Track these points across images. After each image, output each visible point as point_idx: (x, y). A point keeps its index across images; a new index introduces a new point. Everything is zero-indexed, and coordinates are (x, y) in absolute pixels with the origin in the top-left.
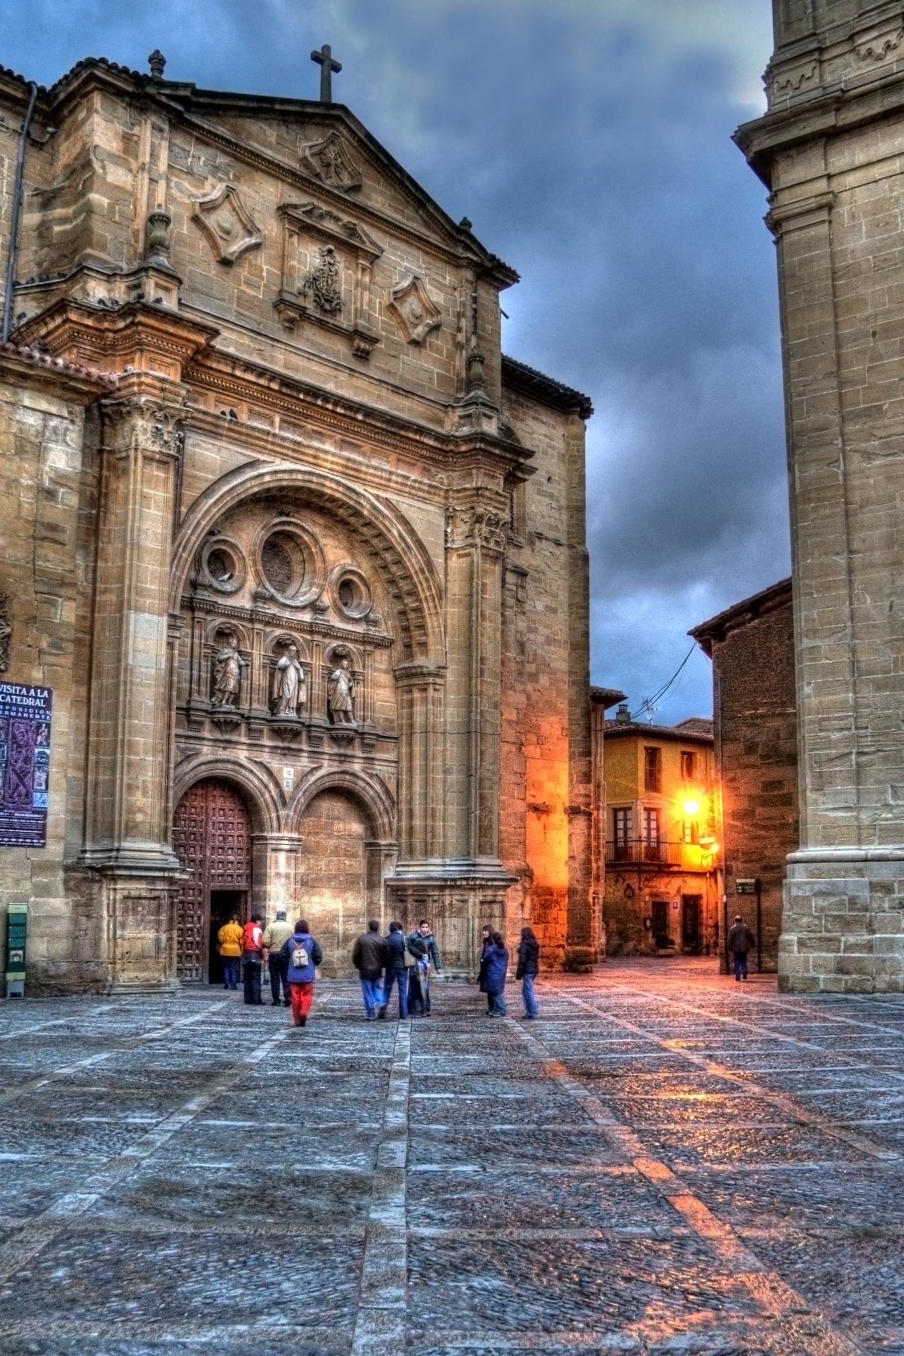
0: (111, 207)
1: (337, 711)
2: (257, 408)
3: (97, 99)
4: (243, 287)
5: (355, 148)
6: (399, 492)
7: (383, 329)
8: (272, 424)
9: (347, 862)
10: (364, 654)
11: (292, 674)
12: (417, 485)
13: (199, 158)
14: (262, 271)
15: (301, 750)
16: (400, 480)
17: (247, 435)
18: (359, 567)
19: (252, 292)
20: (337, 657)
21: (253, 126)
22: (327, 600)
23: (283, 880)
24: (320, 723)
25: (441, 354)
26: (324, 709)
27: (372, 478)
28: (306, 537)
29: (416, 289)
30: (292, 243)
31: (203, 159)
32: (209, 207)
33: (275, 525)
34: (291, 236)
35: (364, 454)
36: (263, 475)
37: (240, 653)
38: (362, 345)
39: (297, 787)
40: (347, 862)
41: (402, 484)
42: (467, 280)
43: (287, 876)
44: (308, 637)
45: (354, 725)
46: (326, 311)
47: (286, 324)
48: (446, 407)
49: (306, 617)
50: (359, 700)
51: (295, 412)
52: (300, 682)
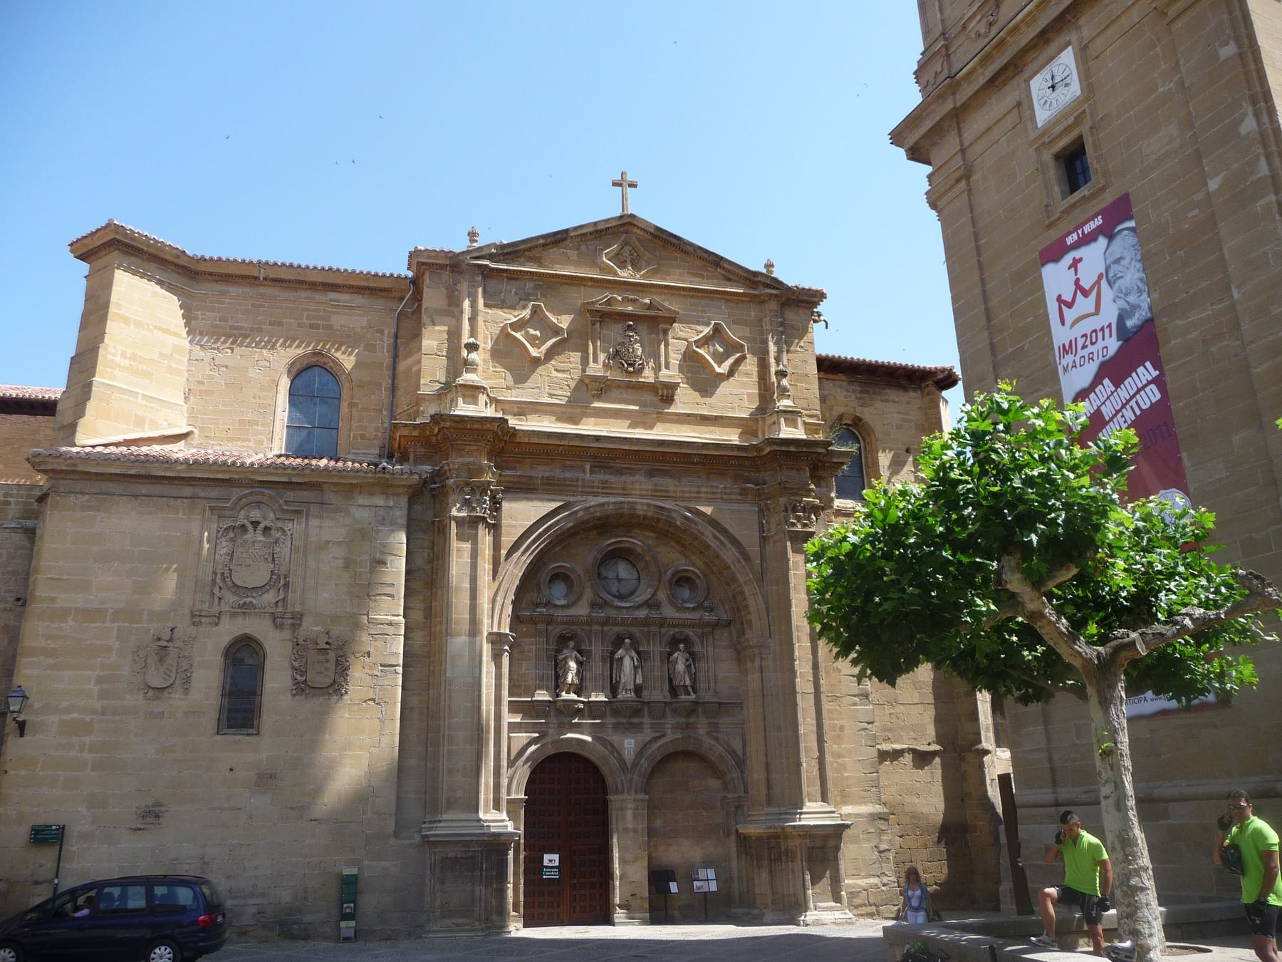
1: (677, 686)
3: (427, 275)
8: (584, 471)
10: (702, 637)
11: (627, 662)
12: (728, 491)
13: (511, 292)
15: (641, 723)
16: (709, 490)
17: (558, 485)
18: (694, 565)
20: (674, 643)
21: (555, 252)
22: (662, 596)
24: (661, 698)
26: (666, 686)
27: (682, 495)
28: (639, 550)
29: (720, 331)
33: (609, 545)
35: (673, 476)
36: (576, 512)
37: (580, 652)
39: (639, 754)
41: (713, 493)
42: (771, 311)
44: (646, 629)
45: (693, 697)
49: (642, 613)
50: (701, 675)
51: (602, 458)
52: (635, 668)
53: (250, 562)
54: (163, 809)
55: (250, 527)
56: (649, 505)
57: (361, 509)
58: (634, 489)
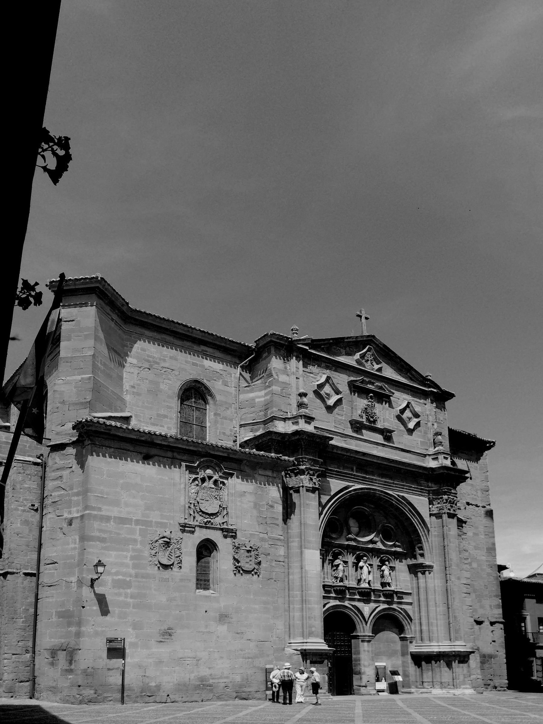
6: (408, 493)
9: (392, 645)
19: (340, 418)
23: (367, 653)
32: (321, 386)
35: (391, 478)
40: (392, 645)
43: (368, 651)
53: (208, 498)
54: (173, 631)
55: (207, 480)
56: (382, 491)
57: (260, 476)
58: (376, 483)
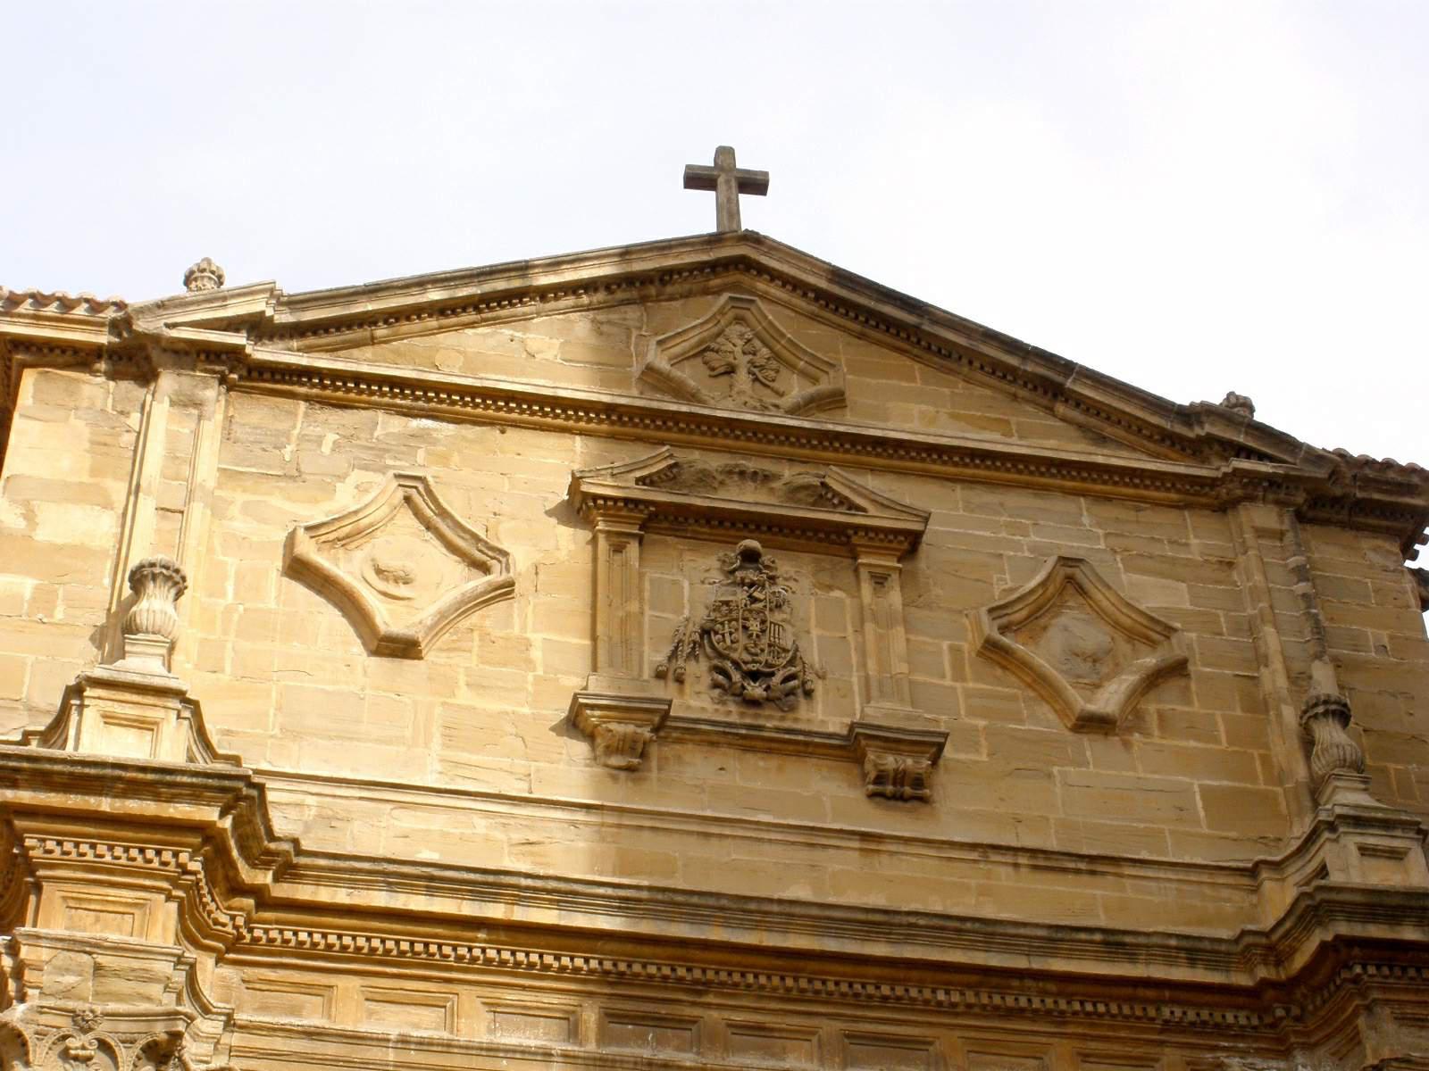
0: (44, 599)
2: (511, 996)
4: (464, 697)
5: (813, 317)
7: (972, 712)
13: (319, 441)
14: (528, 645)
25: (1216, 740)
29: (1082, 591)
30: (625, 564)
31: (331, 438)
34: (618, 549)
38: (890, 762)
46: (754, 703)
47: (615, 761)
48: (1253, 872)
